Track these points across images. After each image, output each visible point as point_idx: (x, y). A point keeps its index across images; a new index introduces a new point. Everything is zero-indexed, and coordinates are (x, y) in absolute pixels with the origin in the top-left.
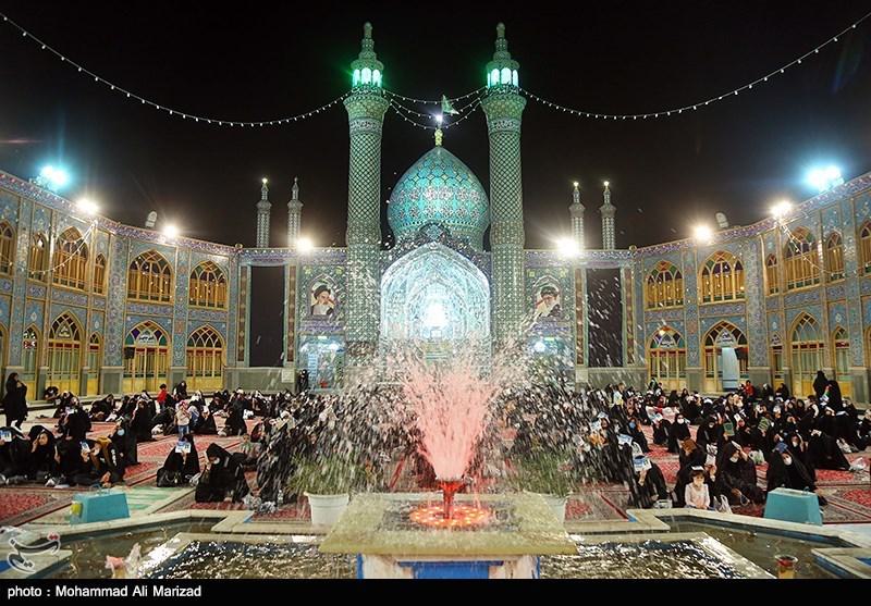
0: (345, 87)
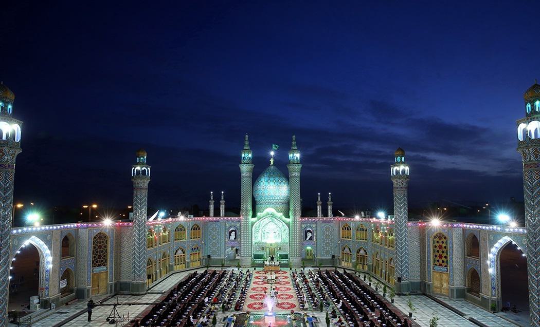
0: (239, 160)
